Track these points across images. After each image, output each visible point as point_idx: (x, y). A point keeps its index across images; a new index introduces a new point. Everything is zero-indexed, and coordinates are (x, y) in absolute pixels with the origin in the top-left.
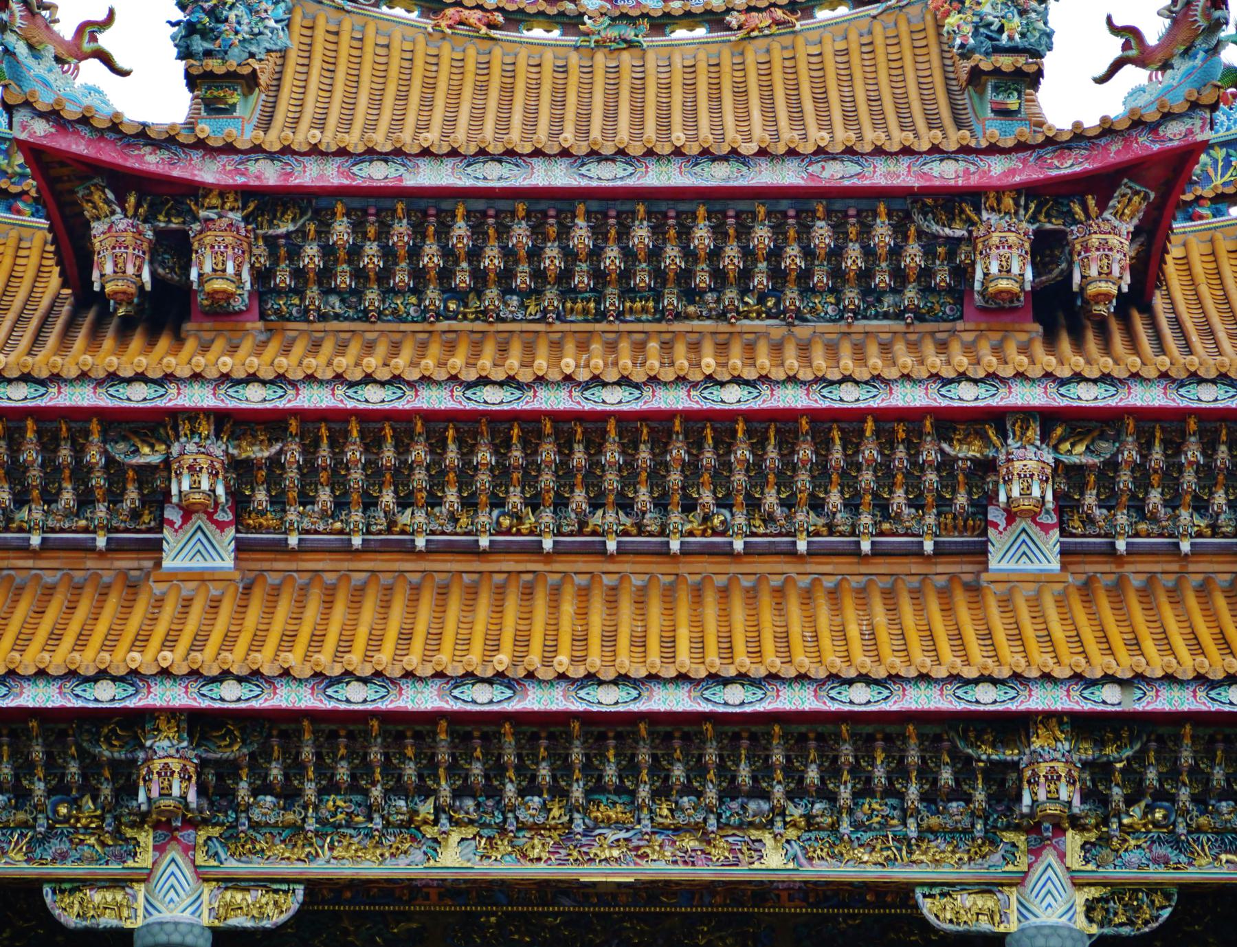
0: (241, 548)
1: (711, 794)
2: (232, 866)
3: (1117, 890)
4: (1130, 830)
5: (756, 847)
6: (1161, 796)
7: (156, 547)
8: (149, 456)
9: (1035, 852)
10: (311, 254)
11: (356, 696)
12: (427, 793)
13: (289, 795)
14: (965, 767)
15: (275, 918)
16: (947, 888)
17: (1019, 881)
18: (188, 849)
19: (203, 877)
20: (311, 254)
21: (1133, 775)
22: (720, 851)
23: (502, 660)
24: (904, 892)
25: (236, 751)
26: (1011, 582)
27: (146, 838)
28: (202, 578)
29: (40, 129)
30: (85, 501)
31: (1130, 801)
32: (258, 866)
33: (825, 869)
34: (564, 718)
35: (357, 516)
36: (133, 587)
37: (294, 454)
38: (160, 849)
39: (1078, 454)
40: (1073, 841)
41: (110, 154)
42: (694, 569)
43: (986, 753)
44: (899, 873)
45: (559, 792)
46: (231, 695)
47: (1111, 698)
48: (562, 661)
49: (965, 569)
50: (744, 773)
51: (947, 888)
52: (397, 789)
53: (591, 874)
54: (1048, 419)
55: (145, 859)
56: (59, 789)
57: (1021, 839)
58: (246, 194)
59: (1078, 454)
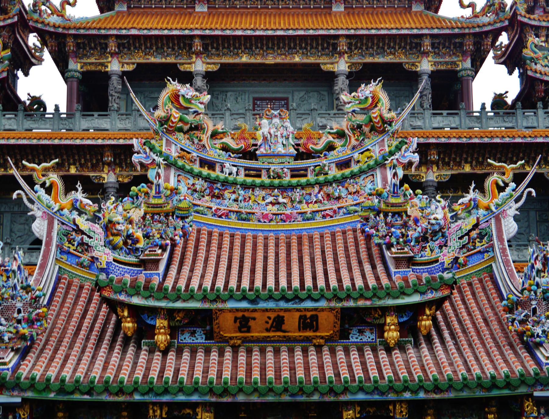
0: (208, 8)
1: (287, 49)
2: (208, 61)
3: (353, 64)
4: (355, 54)
5: (294, 57)
6: (361, 48)
7: (194, 8)
9: (340, 57)
11: (228, 33)
12: (240, 48)
13: (217, 49)
14: (328, 44)
15: (215, 69)
16: (325, 64)
17: (337, 62)
18: (201, 58)
19: (203, 62)
21: (356, 45)
22: (288, 58)
23: (252, 26)
24: (318, 64)
25: (208, 42)
26: (336, 13)
27: (194, 56)
28: (202, 13)
31: (355, 49)
32: (212, 61)
33: (306, 61)
34: (263, 36)
35: (227, 2)
36: (190, 14)
38: (196, 58)
40: (346, 55)
42: (283, 11)
43: (332, 41)
44: (318, 61)
45: (262, 48)
46: (207, 32)
47: (352, 32)
48: (262, 26)
49: (328, 11)
50: (292, 45)
51: (325, 64)
52: (235, 48)
53: (267, 62)
55: (194, 60)
56: (180, 48)
57: (337, 56)
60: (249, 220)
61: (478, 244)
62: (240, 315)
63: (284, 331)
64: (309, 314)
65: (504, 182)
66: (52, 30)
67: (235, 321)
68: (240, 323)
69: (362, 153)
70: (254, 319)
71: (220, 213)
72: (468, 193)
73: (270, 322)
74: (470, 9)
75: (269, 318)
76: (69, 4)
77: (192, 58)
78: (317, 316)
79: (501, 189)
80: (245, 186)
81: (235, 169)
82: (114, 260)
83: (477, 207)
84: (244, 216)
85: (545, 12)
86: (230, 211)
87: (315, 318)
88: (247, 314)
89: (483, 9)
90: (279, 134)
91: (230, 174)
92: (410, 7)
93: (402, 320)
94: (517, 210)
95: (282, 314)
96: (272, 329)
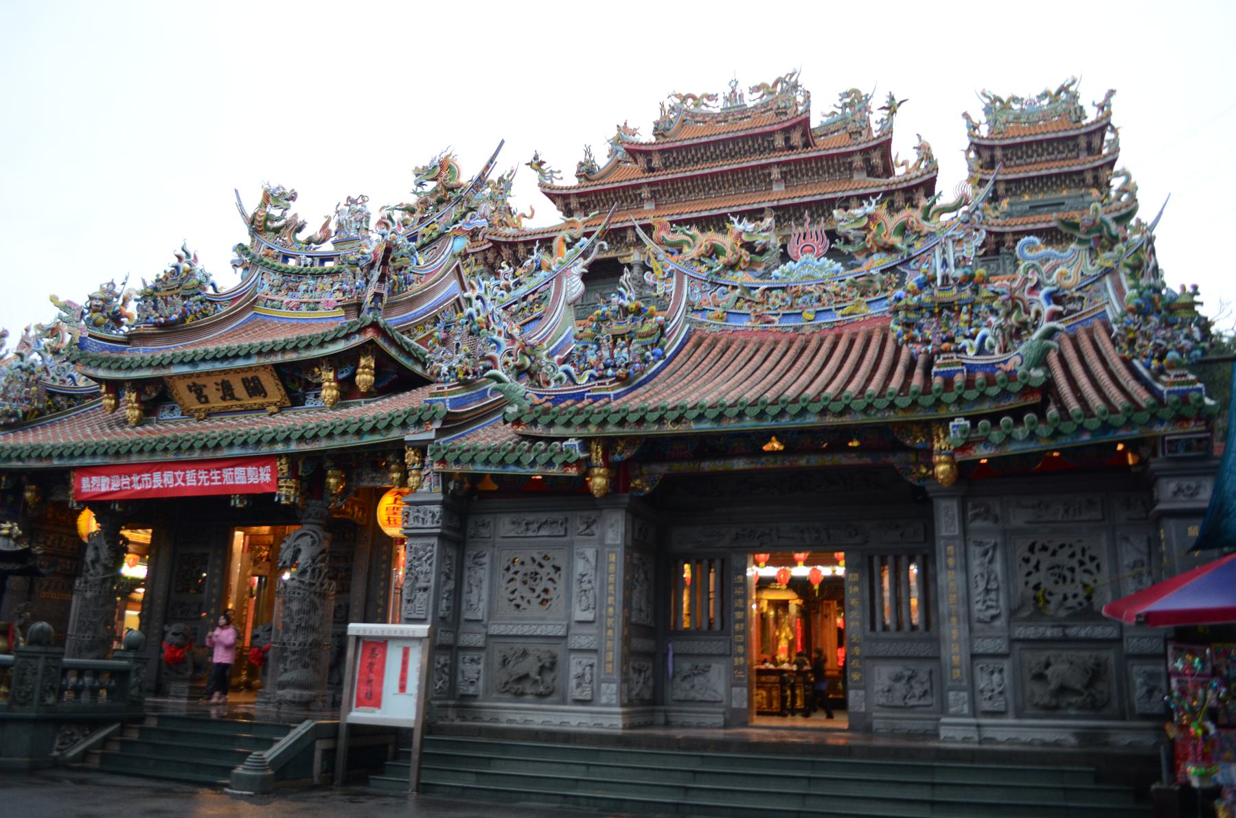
8: (639, 192)
10: (671, 159)
20: (671, 159)
29: (626, 146)
30: (632, 201)
37: (660, 188)
39: (784, 169)
41: (637, 148)
47: (775, 203)
54: (778, 164)
55: (632, 251)
56: (618, 242)
58: (659, 151)
59: (784, 169)
60: (317, 310)
61: (536, 310)
62: (190, 382)
63: (238, 400)
64: (249, 375)
65: (571, 238)
66: (504, 240)
67: (191, 391)
68: (196, 392)
69: (427, 227)
70: (205, 386)
71: (291, 305)
72: (533, 254)
73: (220, 387)
74: (904, 167)
75: (217, 384)
76: (525, 216)
77: (629, 250)
78: (257, 378)
79: (569, 246)
80: (317, 275)
81: (309, 260)
82: (90, 336)
83: (539, 269)
84: (312, 306)
85: (1005, 166)
86: (301, 303)
87: (256, 379)
88: (199, 382)
89: (915, 165)
90: (352, 219)
91: (305, 266)
92: (851, 177)
93: (341, 377)
94: (584, 267)
95: (226, 378)
96: (228, 398)
